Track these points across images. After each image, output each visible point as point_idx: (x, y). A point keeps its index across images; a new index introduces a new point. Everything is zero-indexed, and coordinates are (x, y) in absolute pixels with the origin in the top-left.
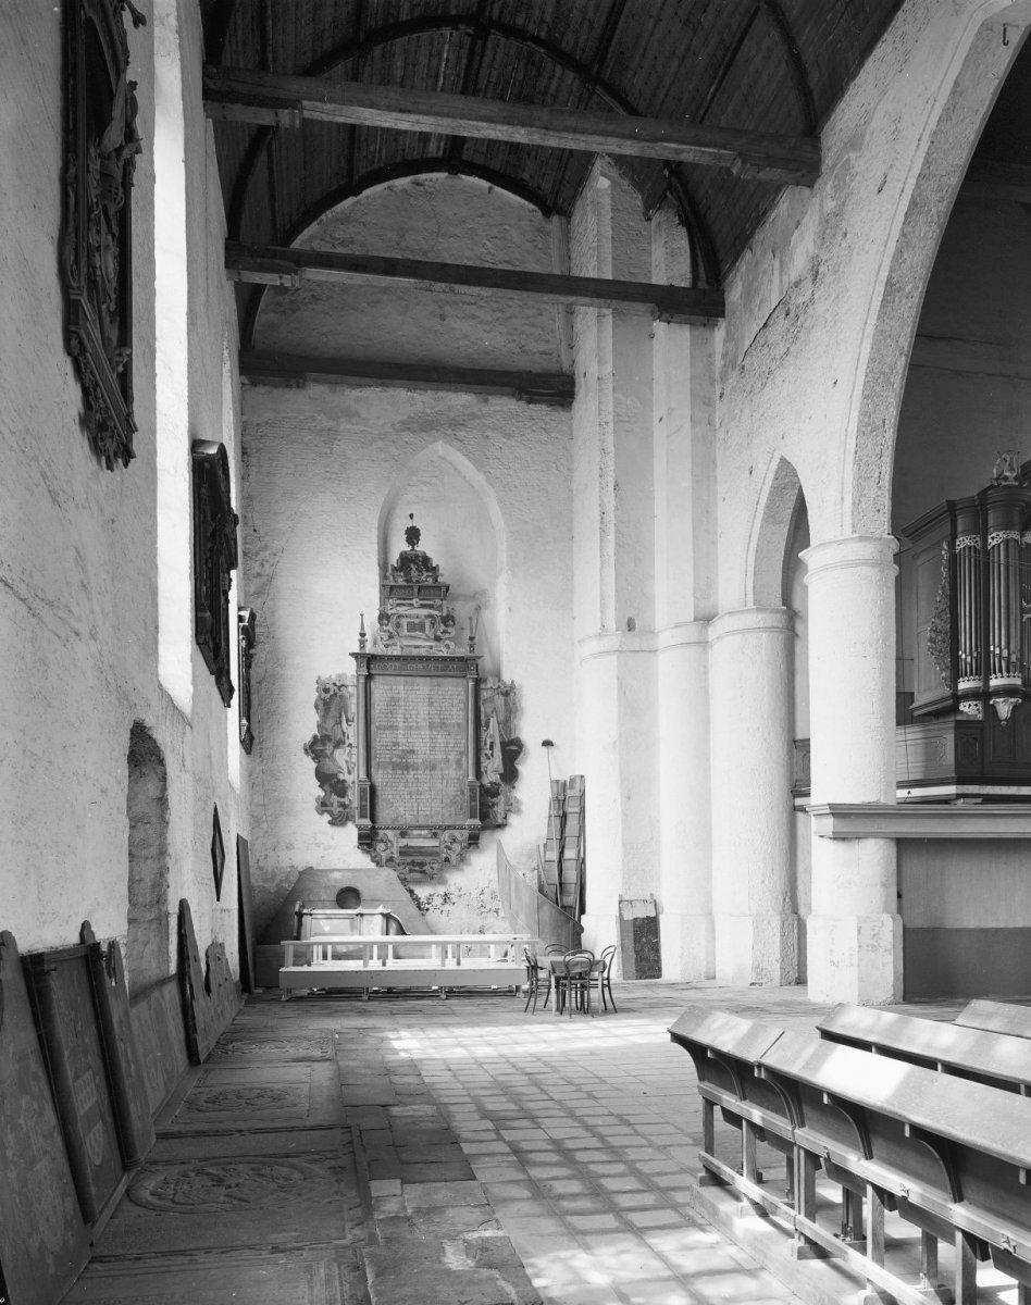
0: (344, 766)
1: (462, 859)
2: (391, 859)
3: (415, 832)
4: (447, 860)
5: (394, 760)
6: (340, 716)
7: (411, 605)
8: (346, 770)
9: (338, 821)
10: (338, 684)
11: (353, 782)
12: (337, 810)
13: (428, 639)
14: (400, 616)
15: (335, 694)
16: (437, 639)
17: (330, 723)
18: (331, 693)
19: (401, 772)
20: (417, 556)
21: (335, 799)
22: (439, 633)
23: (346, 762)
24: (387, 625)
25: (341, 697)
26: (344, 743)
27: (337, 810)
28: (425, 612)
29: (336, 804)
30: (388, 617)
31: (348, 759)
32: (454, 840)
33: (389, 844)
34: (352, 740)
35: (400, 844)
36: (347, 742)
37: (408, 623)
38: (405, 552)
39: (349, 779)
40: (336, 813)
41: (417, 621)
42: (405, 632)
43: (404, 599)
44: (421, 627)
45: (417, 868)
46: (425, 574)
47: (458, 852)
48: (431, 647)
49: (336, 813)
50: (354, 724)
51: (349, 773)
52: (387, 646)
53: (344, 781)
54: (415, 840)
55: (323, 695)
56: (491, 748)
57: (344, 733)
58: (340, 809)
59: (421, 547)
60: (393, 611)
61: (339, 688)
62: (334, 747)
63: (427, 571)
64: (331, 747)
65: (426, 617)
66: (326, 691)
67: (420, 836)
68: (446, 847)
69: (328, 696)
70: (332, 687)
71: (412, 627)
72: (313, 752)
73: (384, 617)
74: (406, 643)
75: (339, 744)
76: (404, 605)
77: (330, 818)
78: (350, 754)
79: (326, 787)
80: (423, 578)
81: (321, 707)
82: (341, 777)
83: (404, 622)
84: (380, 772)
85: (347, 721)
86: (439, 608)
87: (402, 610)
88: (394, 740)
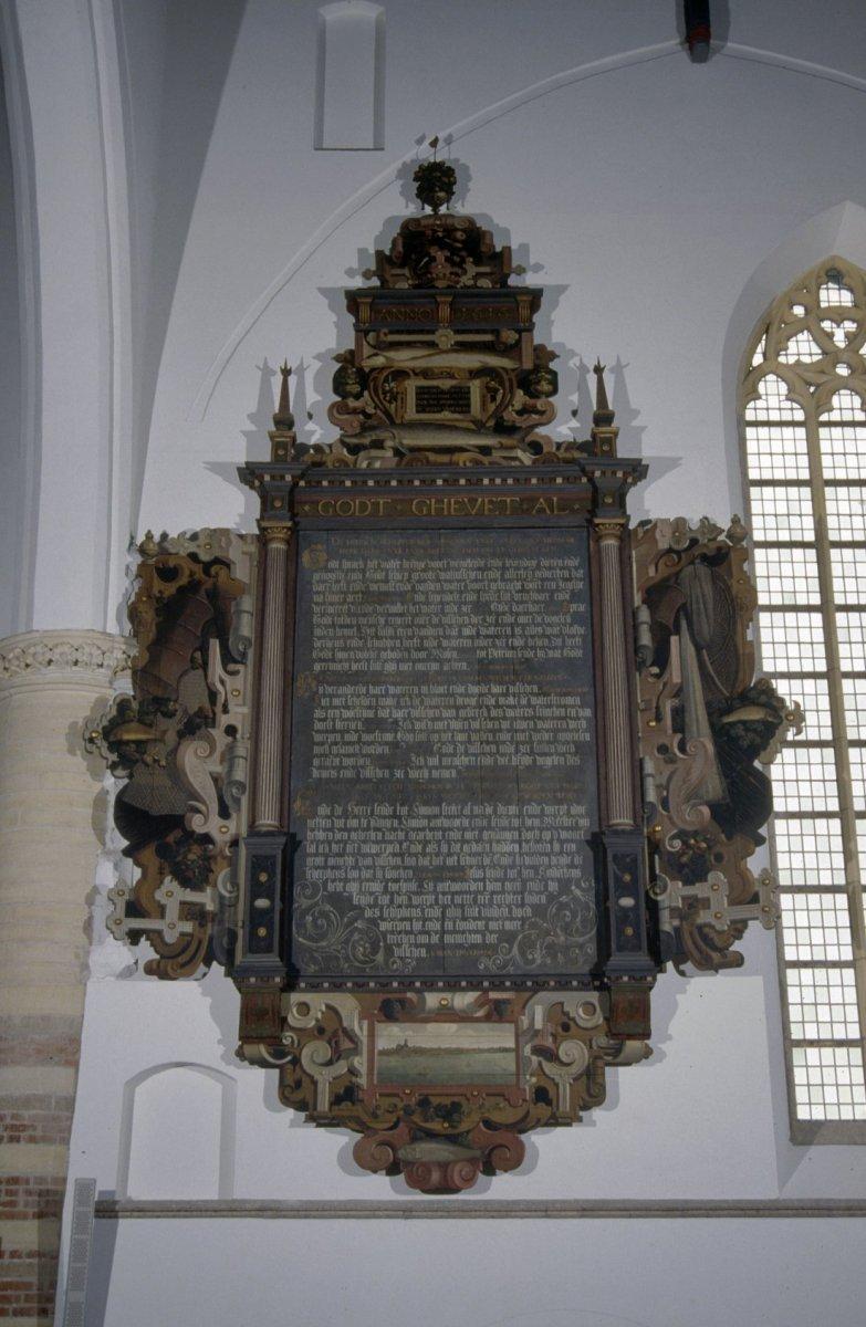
0: (208, 792)
1: (592, 1092)
2: (347, 1094)
3: (432, 1000)
4: (541, 1095)
5: (369, 773)
6: (204, 649)
7: (432, 345)
8: (214, 806)
9: (172, 963)
10: (205, 557)
11: (234, 843)
12: (174, 928)
13: (479, 427)
14: (400, 375)
15: (194, 586)
16: (502, 428)
17: (169, 669)
18: (183, 580)
19: (386, 810)
20: (450, 231)
21: (171, 893)
22: (510, 416)
23: (216, 779)
24: (358, 396)
25: (214, 595)
26: (213, 723)
27: (174, 928)
28: (473, 360)
29: (173, 911)
30: (364, 378)
31: (218, 769)
32: (566, 1026)
33: (346, 1044)
34: (239, 714)
35: (381, 1044)
36: (224, 720)
37: (421, 391)
38: (416, 221)
39: (220, 830)
40: (171, 937)
41: (446, 384)
42: (411, 413)
43: (409, 332)
44: (459, 399)
45: (436, 1126)
46: (472, 269)
47: (575, 1069)
48: (485, 450)
49: (171, 937)
50: (245, 673)
51: (224, 813)
52: (354, 450)
53: (206, 839)
54: (431, 1027)
55: (158, 585)
56: (680, 726)
57: (213, 695)
58: (188, 927)
59: (467, 204)
60: (379, 361)
61: (207, 567)
62: (181, 735)
63: (477, 263)
64: (171, 737)
65: (474, 374)
66: (168, 573)
67: (447, 1014)
68: (538, 1051)
69: (170, 589)
70: (187, 566)
71: (430, 400)
72: (115, 746)
73: (351, 377)
74: (411, 439)
75: (197, 724)
76: (409, 345)
77: (151, 955)
78: (229, 757)
79: (149, 854)
80: (466, 280)
81: (149, 615)
82: (197, 824)
83: (411, 385)
84: (323, 810)
85: (227, 658)
86: (512, 350)
87: (403, 358)
88: (370, 714)
